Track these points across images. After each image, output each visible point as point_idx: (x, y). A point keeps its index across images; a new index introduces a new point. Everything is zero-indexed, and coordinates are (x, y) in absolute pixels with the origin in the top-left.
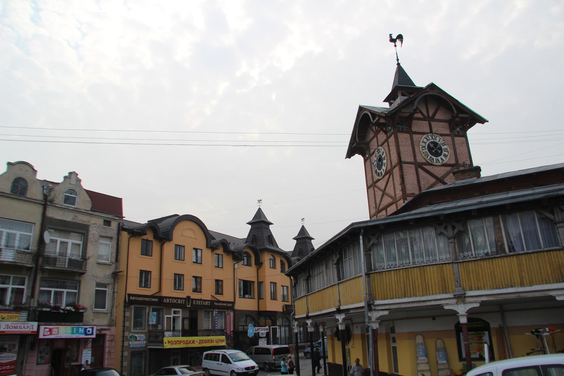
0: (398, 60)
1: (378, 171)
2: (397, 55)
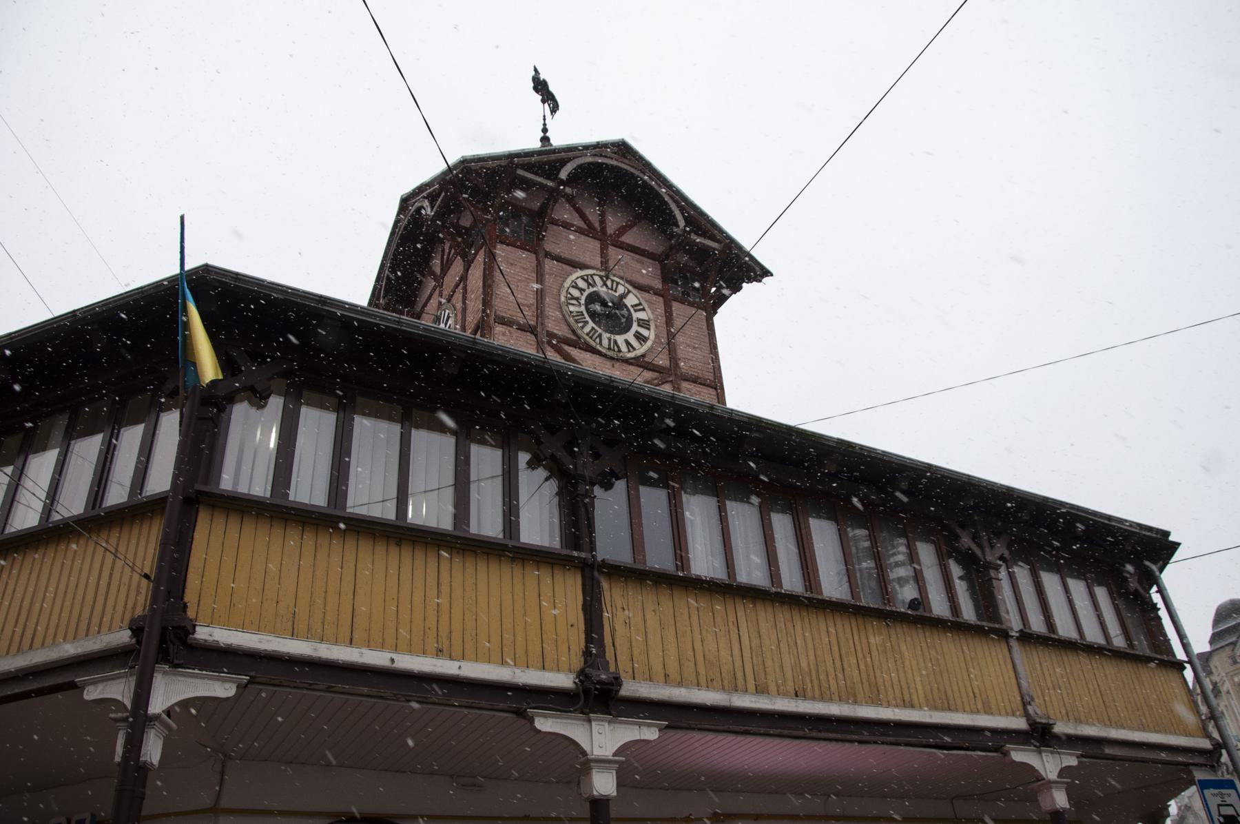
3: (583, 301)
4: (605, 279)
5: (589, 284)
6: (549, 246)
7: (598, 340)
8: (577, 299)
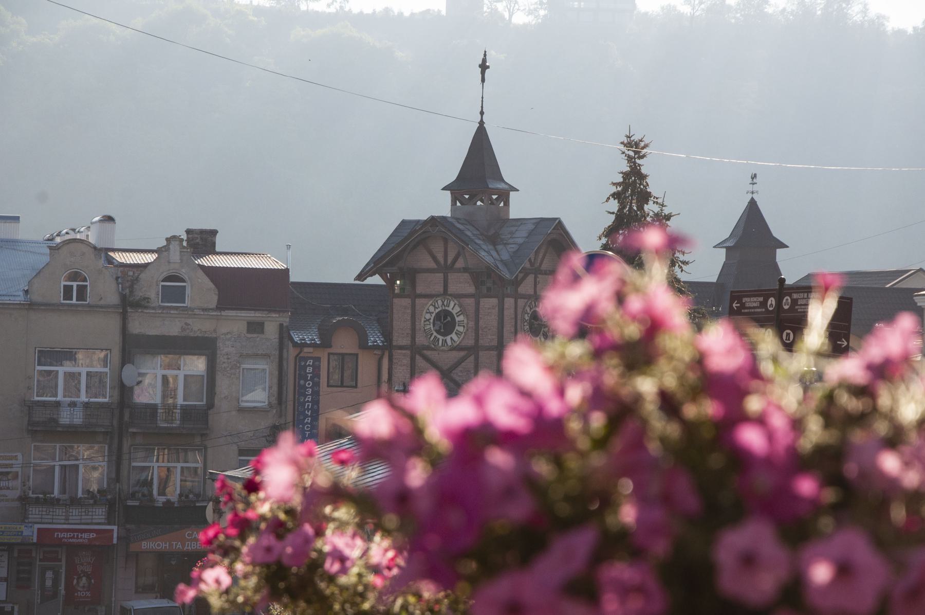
0: (482, 113)
1: (435, 334)
2: (482, 101)
3: (432, 321)
4: (443, 300)
5: (434, 306)
6: (420, 290)
7: (437, 343)
8: (429, 320)
